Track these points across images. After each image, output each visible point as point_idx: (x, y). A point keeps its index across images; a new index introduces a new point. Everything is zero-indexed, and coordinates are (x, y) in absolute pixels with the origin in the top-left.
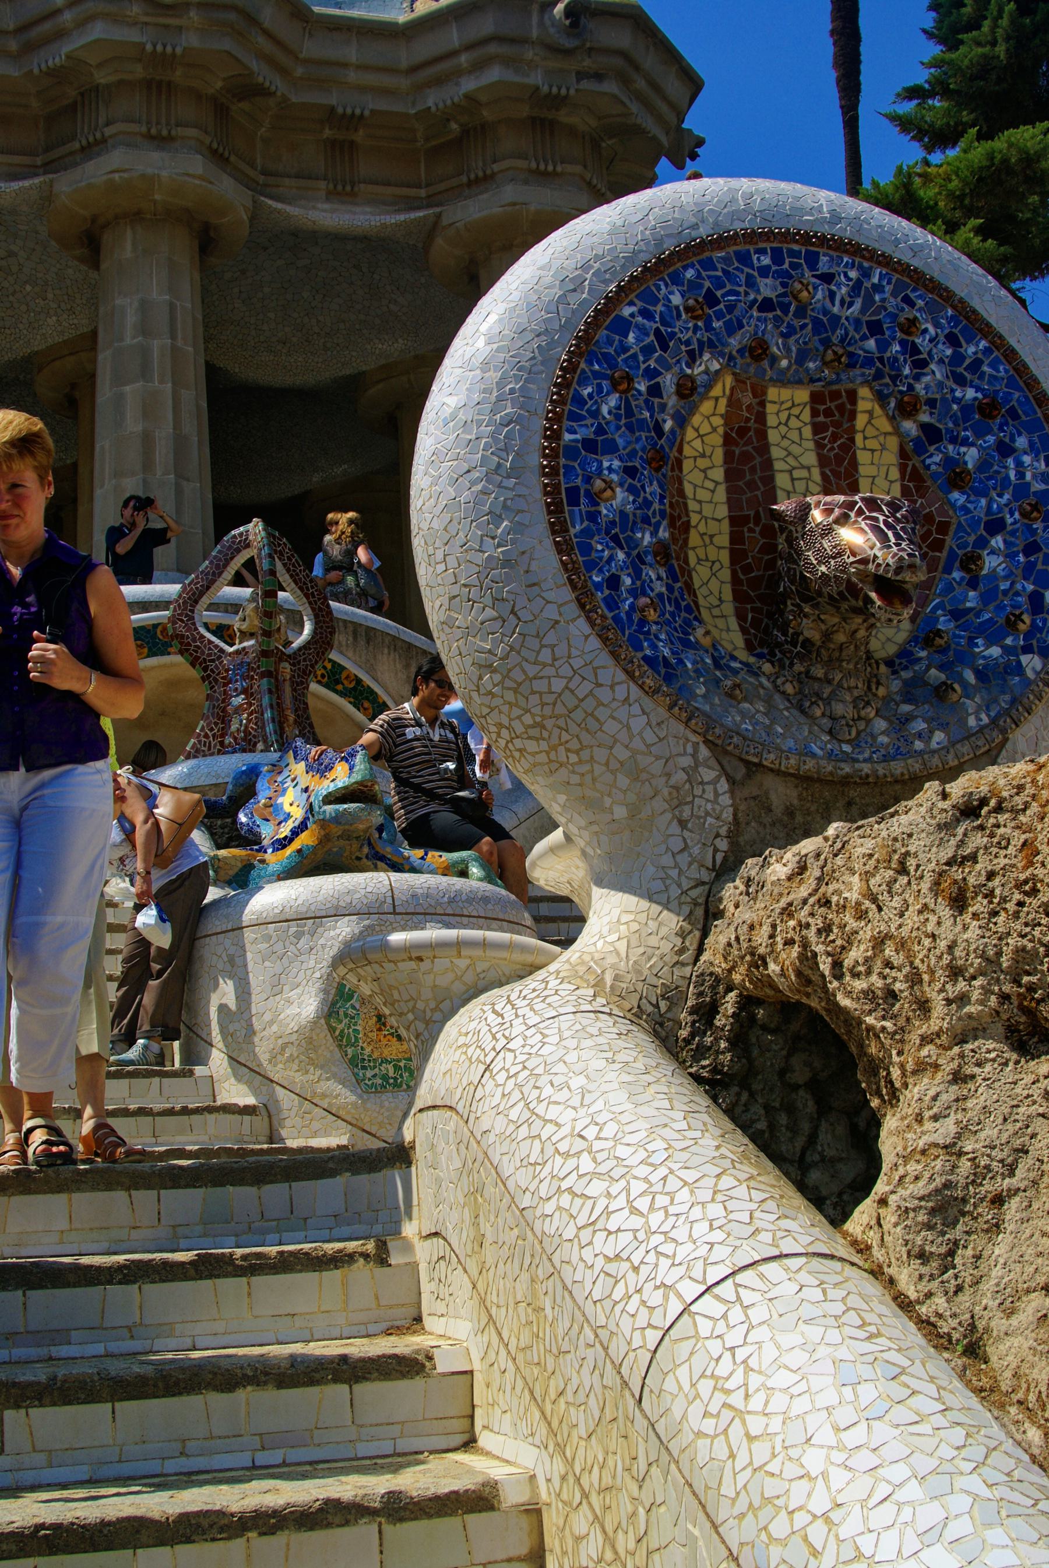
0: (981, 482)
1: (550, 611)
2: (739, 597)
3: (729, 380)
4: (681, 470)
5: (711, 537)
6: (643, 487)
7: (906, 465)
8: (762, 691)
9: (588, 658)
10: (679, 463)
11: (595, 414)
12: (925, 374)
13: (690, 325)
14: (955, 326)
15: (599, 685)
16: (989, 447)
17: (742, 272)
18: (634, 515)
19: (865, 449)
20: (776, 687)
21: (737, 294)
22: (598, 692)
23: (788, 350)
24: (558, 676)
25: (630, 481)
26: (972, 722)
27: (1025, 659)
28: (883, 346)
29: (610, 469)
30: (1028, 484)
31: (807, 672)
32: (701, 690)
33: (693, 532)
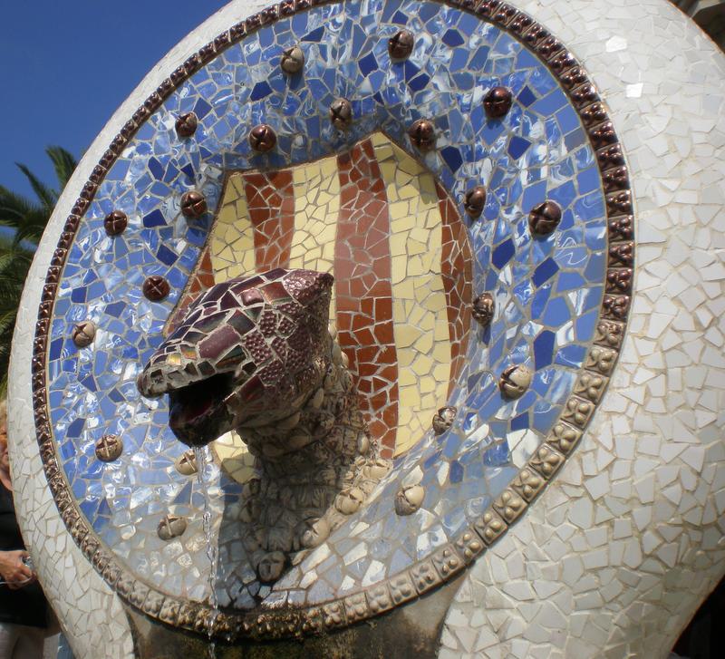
3: (237, 180)
6: (129, 321)
12: (427, 93)
14: (454, 22)
19: (399, 200)
21: (227, 92)
23: (298, 126)
26: (423, 543)
27: (513, 438)
28: (376, 81)
30: (544, 183)
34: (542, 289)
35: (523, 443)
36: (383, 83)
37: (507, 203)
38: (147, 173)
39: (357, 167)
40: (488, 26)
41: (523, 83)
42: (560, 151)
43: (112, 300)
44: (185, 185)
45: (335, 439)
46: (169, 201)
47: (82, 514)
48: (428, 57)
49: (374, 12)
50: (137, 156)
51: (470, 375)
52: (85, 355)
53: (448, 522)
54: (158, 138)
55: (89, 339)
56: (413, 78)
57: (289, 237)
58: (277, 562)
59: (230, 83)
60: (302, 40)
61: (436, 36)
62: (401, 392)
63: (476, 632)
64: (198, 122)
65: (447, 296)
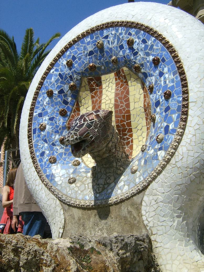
3: (86, 80)
6: (56, 122)
12: (138, 57)
18: (52, 132)
23: (102, 64)
26: (137, 180)
27: (159, 153)
28: (124, 52)
34: (167, 114)
35: (161, 154)
36: (126, 53)
38: (58, 78)
40: (153, 38)
41: (162, 56)
42: (171, 76)
43: (50, 116)
44: (70, 81)
45: (115, 154)
46: (65, 86)
47: (46, 178)
49: (123, 31)
50: (55, 72)
51: (150, 136)
53: (144, 175)
55: (45, 128)
56: (134, 52)
57: (100, 97)
58: (101, 187)
59: (82, 51)
60: (102, 38)
61: (140, 40)
62: (134, 140)
63: (150, 201)
64: (73, 62)
65: (145, 114)
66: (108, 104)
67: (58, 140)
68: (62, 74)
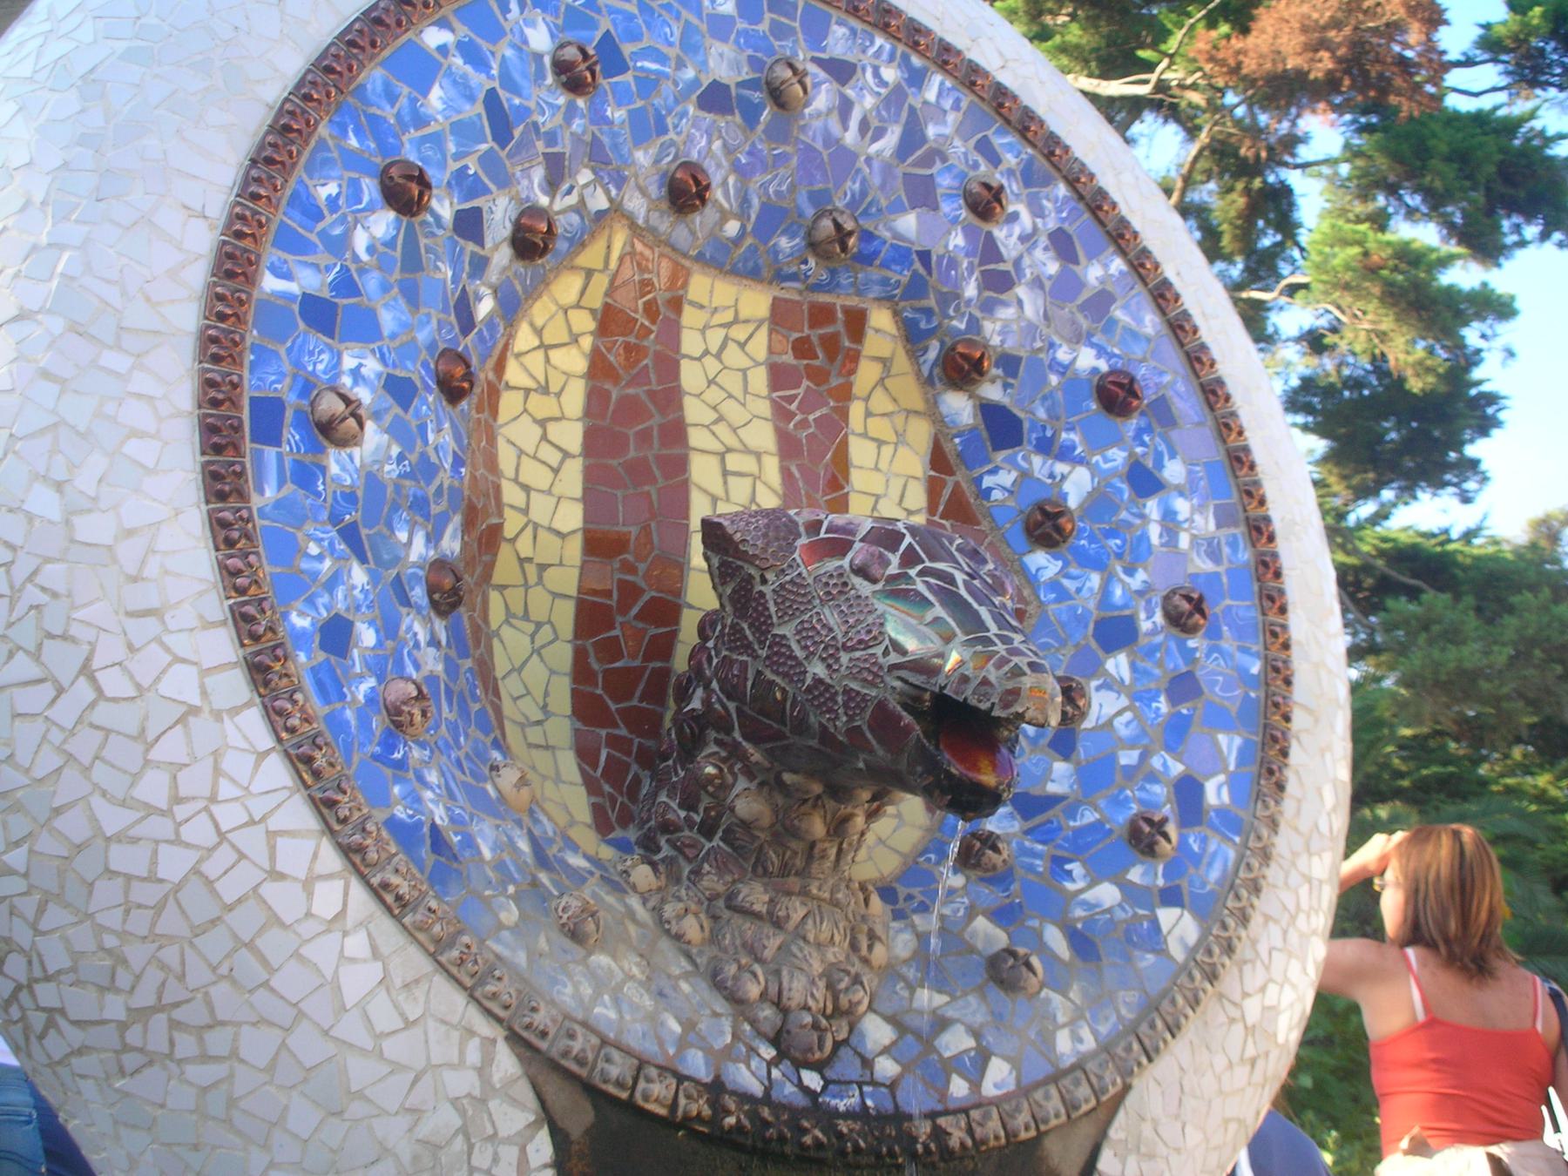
0: (1092, 539)
1: (182, 685)
2: (586, 709)
4: (495, 413)
5: (543, 567)
6: (422, 429)
7: (944, 484)
8: (632, 929)
9: (258, 808)
10: (493, 394)
11: (339, 246)
13: (561, 101)
15: (276, 875)
16: (1114, 472)
17: (678, 18)
18: (398, 488)
19: (865, 435)
20: (661, 921)
22: (270, 890)
23: (745, 201)
24: (177, 841)
25: (398, 410)
26: (1064, 1043)
27: (1166, 916)
29: (356, 373)
31: (730, 898)
32: (510, 914)
33: (505, 551)
37: (1127, 558)
38: (479, 115)
39: (815, 340)
40: (1118, 265)
48: (1021, 247)
50: (458, 61)
52: (344, 469)
54: (509, 53)
56: (992, 266)
59: (670, 44)
60: (814, 60)
61: (1039, 221)
66: (748, 481)
67: (421, 573)
68: (506, 106)
